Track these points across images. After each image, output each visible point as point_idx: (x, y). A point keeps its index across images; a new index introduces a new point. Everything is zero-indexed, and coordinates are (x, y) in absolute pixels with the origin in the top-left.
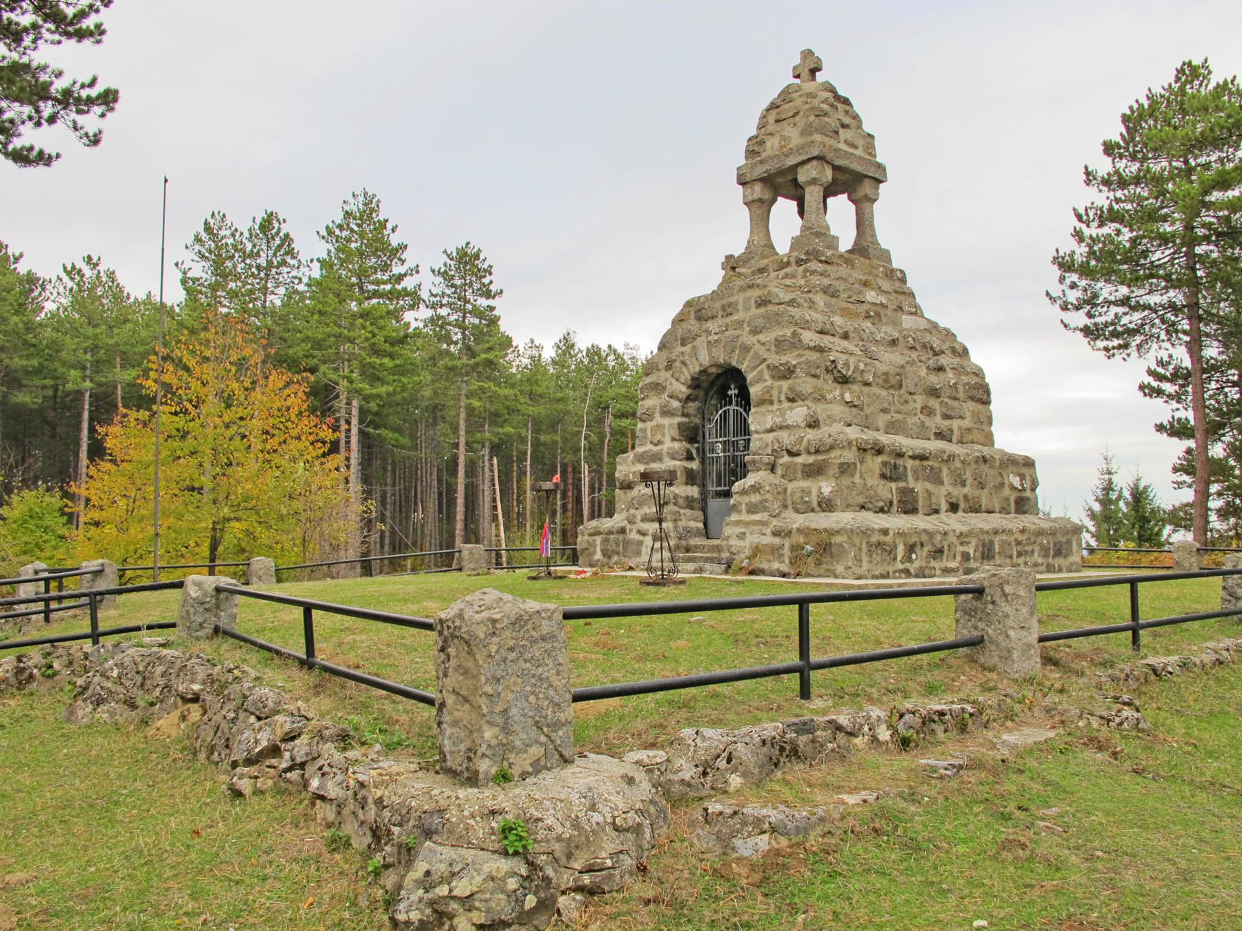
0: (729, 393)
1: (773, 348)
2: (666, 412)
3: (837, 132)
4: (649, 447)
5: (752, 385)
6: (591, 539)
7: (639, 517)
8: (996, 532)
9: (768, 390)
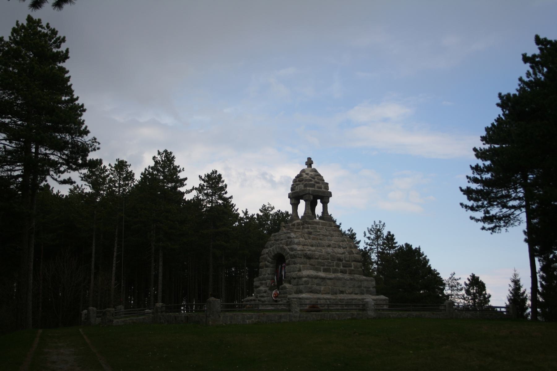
2: (267, 266)
3: (315, 185)
8: (353, 299)
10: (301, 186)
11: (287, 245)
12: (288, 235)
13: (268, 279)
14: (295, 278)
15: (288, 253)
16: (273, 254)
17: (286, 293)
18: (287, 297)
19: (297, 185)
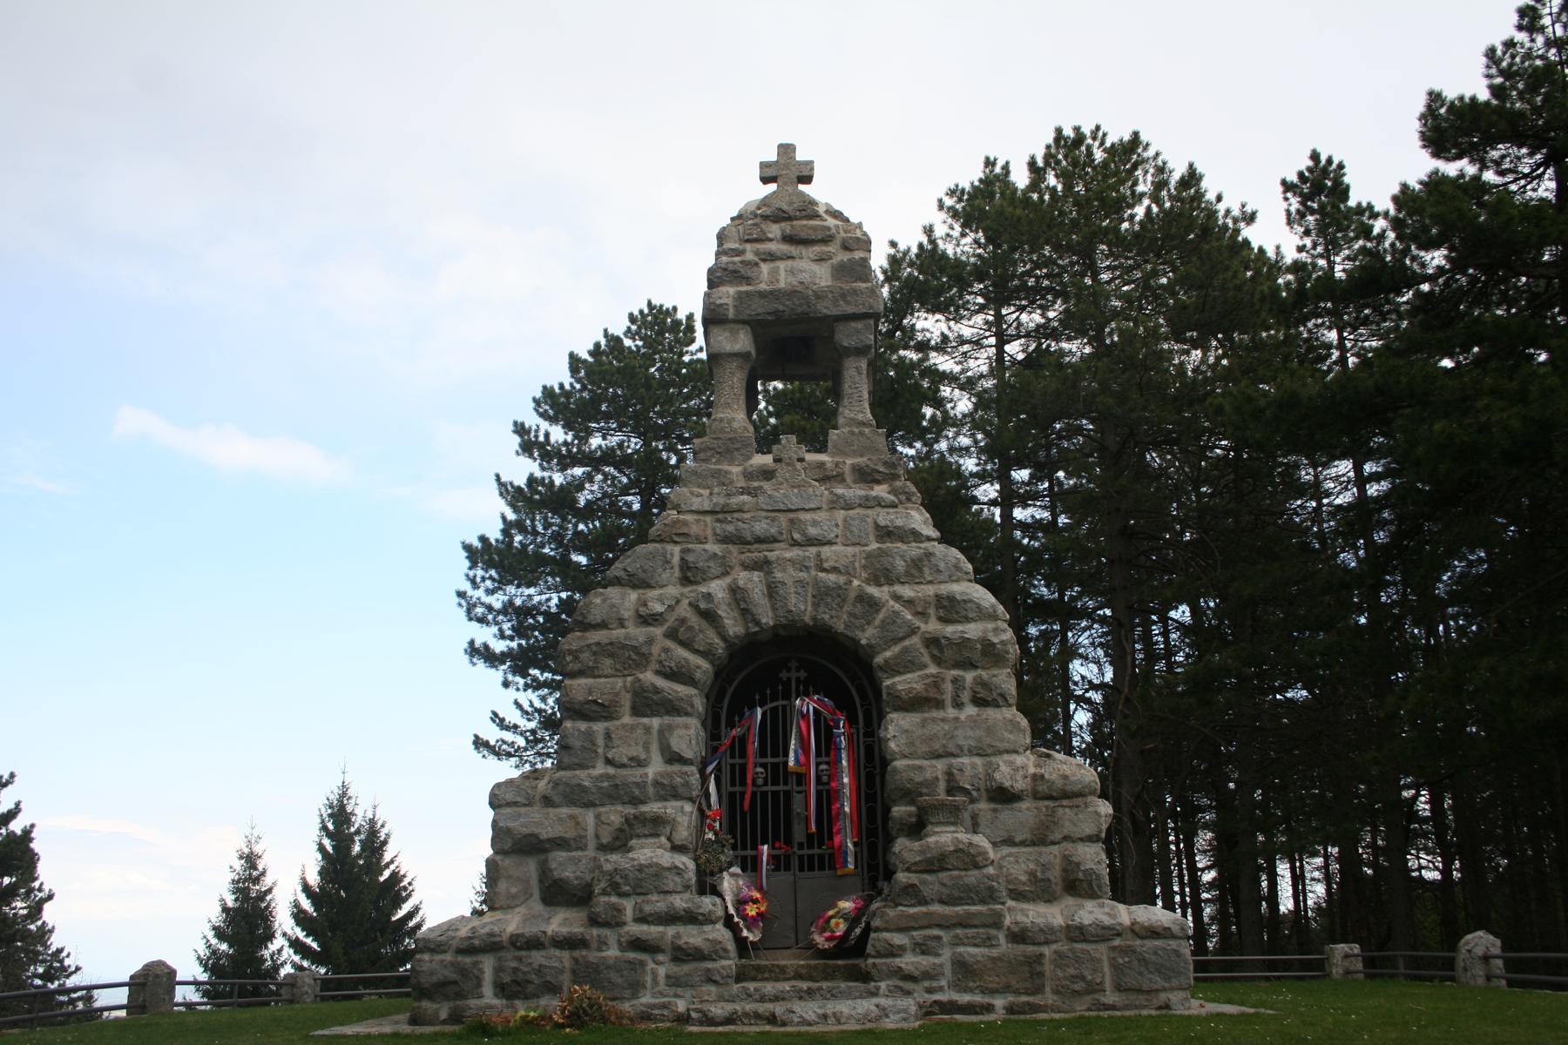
0: (784, 675)
1: (932, 611)
2: (647, 703)
4: (600, 769)
5: (893, 668)
6: (468, 960)
7: (629, 913)
9: (936, 683)
10: (810, 272)
11: (882, 576)
12: (884, 517)
13: (669, 792)
14: (1003, 796)
15: (913, 631)
16: (734, 626)
17: (989, 896)
18: (996, 923)
19: (771, 257)
